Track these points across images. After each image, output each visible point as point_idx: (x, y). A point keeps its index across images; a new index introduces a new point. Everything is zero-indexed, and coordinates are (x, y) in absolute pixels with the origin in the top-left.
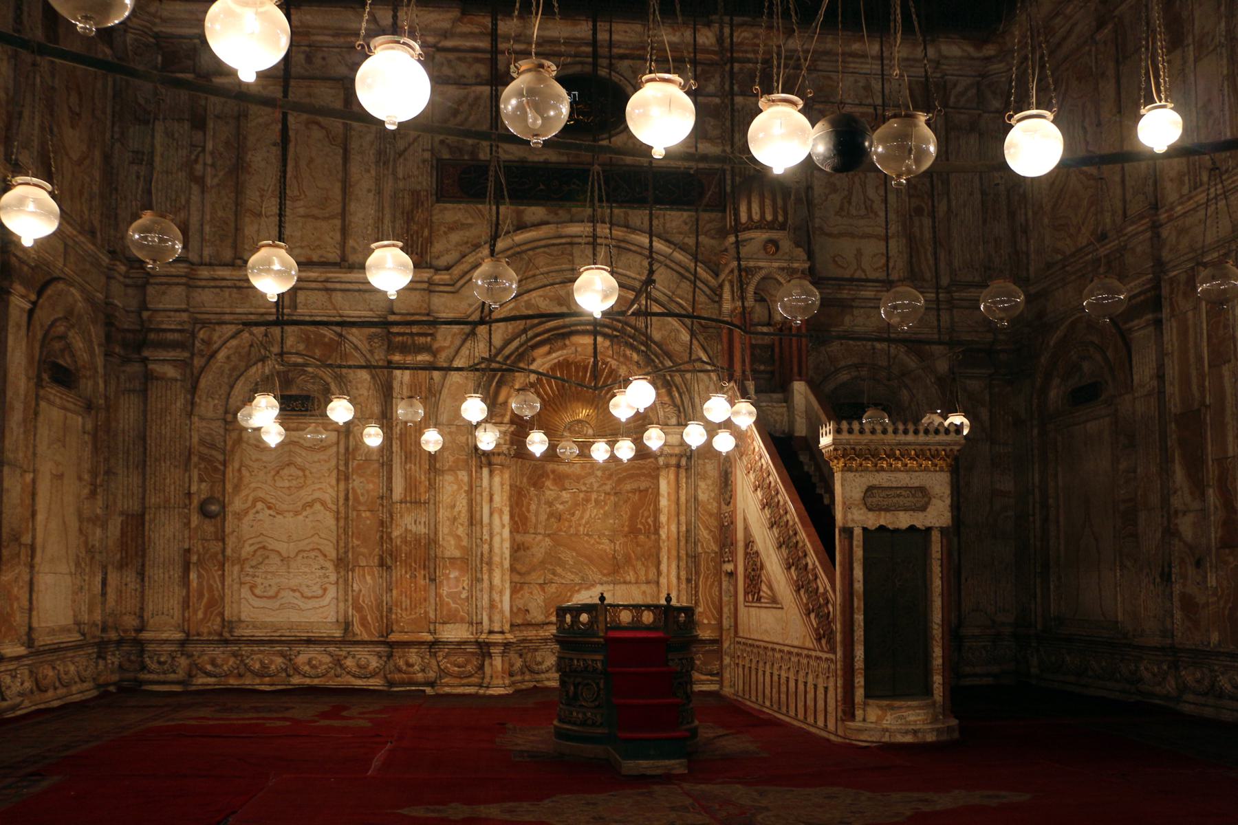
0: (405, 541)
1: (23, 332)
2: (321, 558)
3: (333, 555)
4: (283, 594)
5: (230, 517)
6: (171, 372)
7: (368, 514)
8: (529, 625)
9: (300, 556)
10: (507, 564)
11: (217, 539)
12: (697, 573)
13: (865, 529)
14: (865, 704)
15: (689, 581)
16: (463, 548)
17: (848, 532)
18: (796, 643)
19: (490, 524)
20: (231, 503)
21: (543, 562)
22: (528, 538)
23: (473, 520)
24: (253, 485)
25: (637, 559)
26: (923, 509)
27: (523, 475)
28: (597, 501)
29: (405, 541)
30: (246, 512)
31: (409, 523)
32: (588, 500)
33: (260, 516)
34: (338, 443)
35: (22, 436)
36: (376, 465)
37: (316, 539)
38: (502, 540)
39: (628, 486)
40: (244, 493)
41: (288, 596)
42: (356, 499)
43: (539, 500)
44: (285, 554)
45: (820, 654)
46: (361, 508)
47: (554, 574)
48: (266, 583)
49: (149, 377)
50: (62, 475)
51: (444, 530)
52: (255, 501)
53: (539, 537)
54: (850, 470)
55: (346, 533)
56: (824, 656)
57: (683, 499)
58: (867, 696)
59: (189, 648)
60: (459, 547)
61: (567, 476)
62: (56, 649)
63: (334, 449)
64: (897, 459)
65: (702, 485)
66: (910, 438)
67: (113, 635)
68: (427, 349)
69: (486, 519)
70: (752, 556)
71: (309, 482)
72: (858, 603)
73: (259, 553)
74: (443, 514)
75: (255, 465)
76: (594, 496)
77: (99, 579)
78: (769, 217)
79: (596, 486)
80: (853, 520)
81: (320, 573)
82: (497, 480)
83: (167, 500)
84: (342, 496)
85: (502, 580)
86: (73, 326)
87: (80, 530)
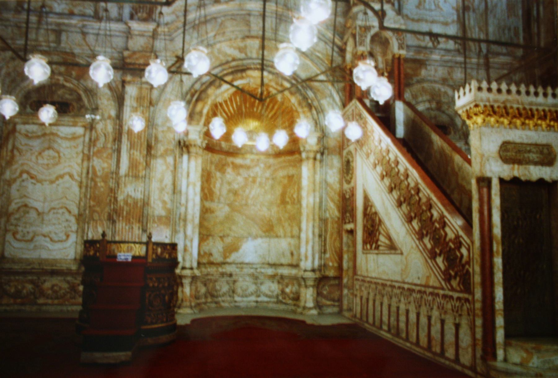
2: (67, 214)
3: (75, 211)
4: (37, 238)
7: (102, 184)
8: (211, 263)
9: (52, 211)
10: (197, 221)
12: (326, 231)
15: (320, 236)
17: (484, 182)
18: (418, 282)
19: (187, 194)
23: (175, 190)
24: (20, 162)
28: (260, 184)
29: (126, 203)
30: (15, 180)
32: (254, 181)
33: (24, 184)
34: (84, 135)
36: (110, 151)
37: (64, 200)
38: (194, 205)
39: (281, 173)
40: (14, 167)
42: (95, 173)
43: (222, 181)
44: (40, 210)
45: (451, 293)
46: (98, 180)
53: (221, 206)
55: (85, 196)
56: (455, 295)
58: (507, 336)
60: (164, 208)
61: (241, 166)
63: (81, 139)
69: (184, 189)
71: (62, 160)
72: (497, 247)
73: (22, 209)
74: (155, 185)
76: (258, 180)
80: (491, 171)
81: (66, 224)
82: (193, 163)
84: (85, 171)
85: (193, 232)
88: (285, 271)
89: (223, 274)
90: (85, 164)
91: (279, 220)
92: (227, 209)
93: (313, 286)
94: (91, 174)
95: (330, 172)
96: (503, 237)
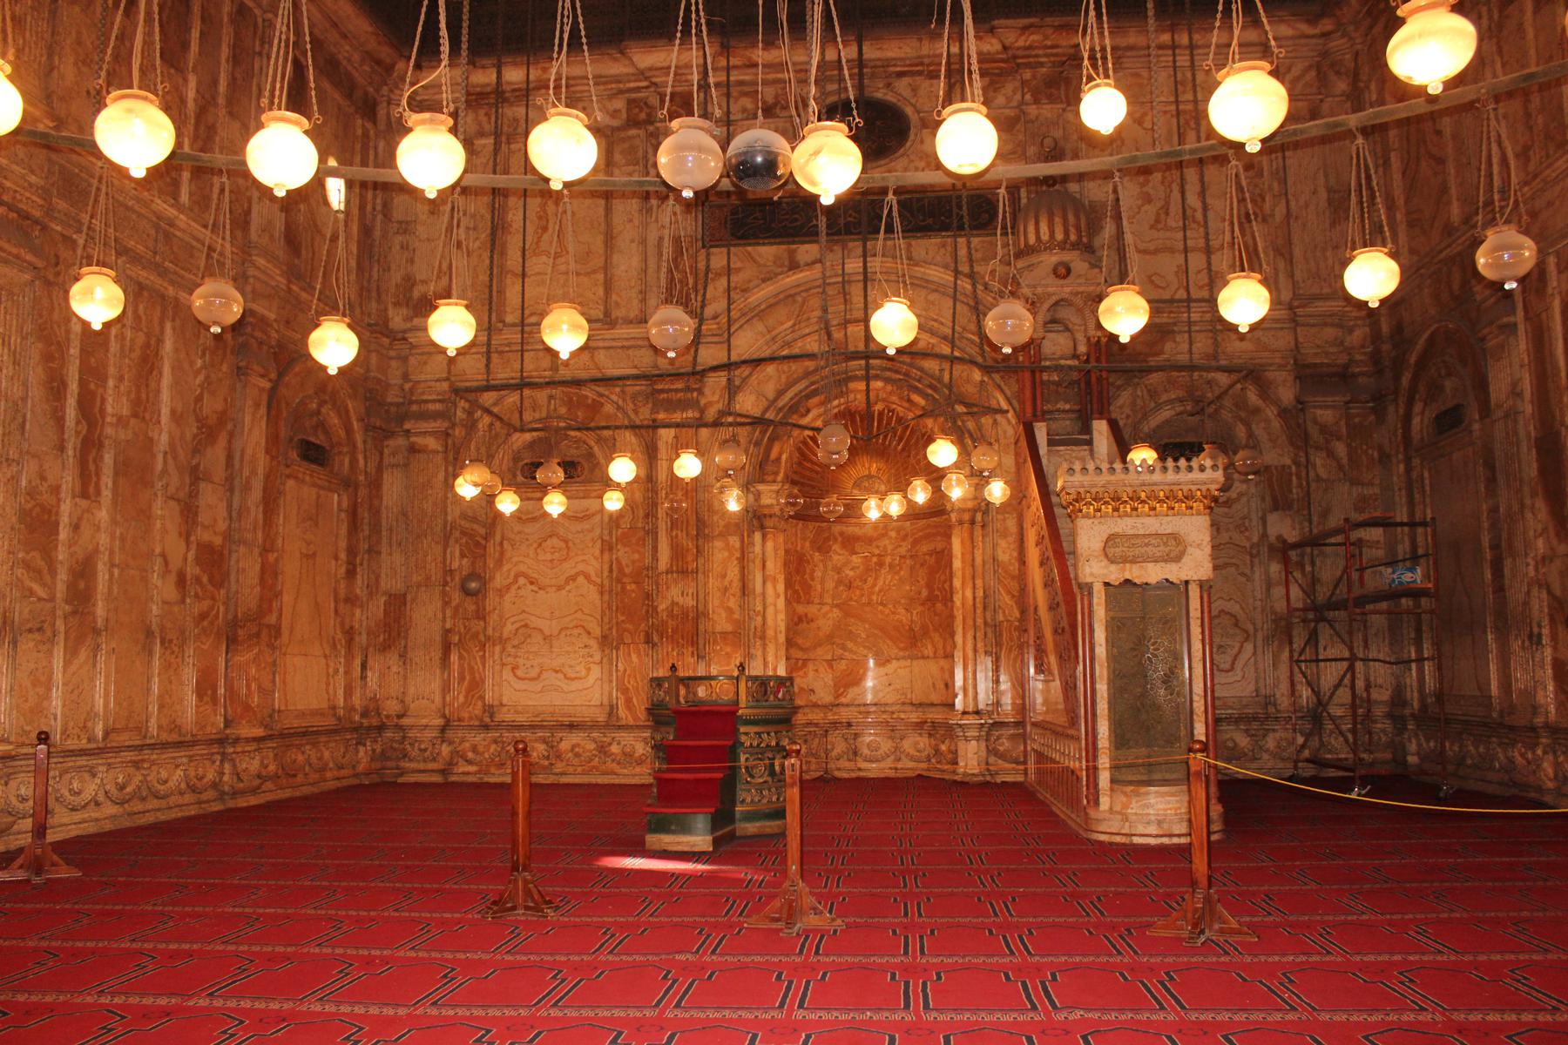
0: (671, 615)
1: (263, 410)
2: (584, 635)
3: (597, 631)
4: (545, 675)
5: (491, 595)
6: (432, 443)
7: (633, 586)
10: (782, 638)
11: (478, 618)
13: (1107, 584)
14: (1112, 790)
16: (737, 622)
19: (764, 594)
20: (492, 578)
21: (830, 638)
22: (812, 610)
23: (745, 589)
24: (515, 559)
25: (936, 630)
26: (1178, 559)
27: (804, 539)
30: (508, 588)
31: (676, 595)
32: (881, 564)
33: (522, 592)
35: (261, 516)
36: (641, 533)
38: (776, 612)
39: (925, 548)
41: (551, 678)
42: (621, 570)
43: (825, 567)
47: (844, 648)
48: (529, 664)
49: (413, 449)
50: (314, 554)
51: (714, 602)
52: (517, 576)
54: (1087, 516)
55: (610, 608)
57: (979, 560)
59: (450, 734)
62: (308, 735)
64: (1143, 502)
65: (1003, 543)
66: (1184, 476)
67: (375, 722)
68: (694, 404)
70: (1038, 621)
74: (713, 583)
75: (517, 538)
76: (888, 560)
77: (358, 662)
78: (1059, 236)
79: (890, 548)
80: (1092, 574)
82: (770, 545)
83: (428, 578)
84: (606, 567)
86: (325, 402)
87: (336, 611)
88: (936, 715)
89: (835, 725)
90: (606, 556)
91: (924, 627)
92: (836, 613)
93: (978, 739)
94: (617, 574)
95: (1003, 543)
96: (1111, 657)
